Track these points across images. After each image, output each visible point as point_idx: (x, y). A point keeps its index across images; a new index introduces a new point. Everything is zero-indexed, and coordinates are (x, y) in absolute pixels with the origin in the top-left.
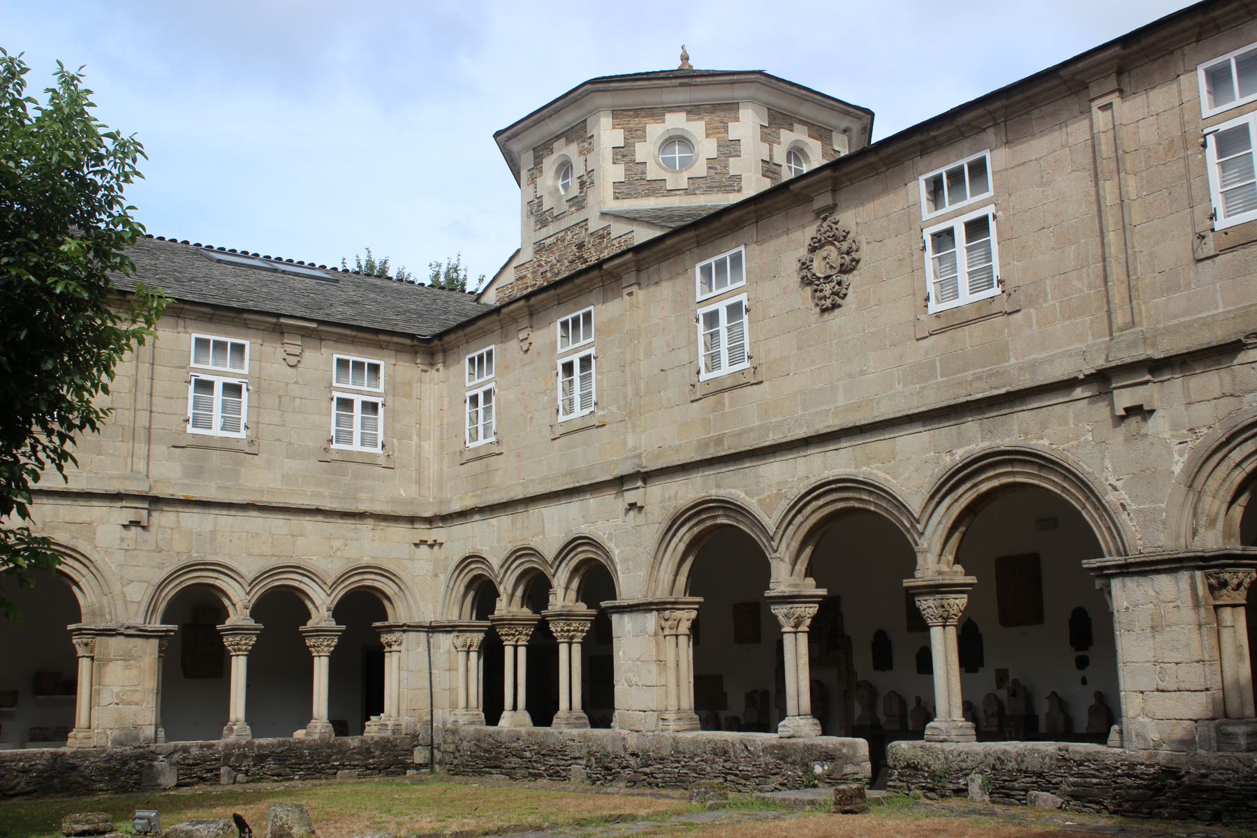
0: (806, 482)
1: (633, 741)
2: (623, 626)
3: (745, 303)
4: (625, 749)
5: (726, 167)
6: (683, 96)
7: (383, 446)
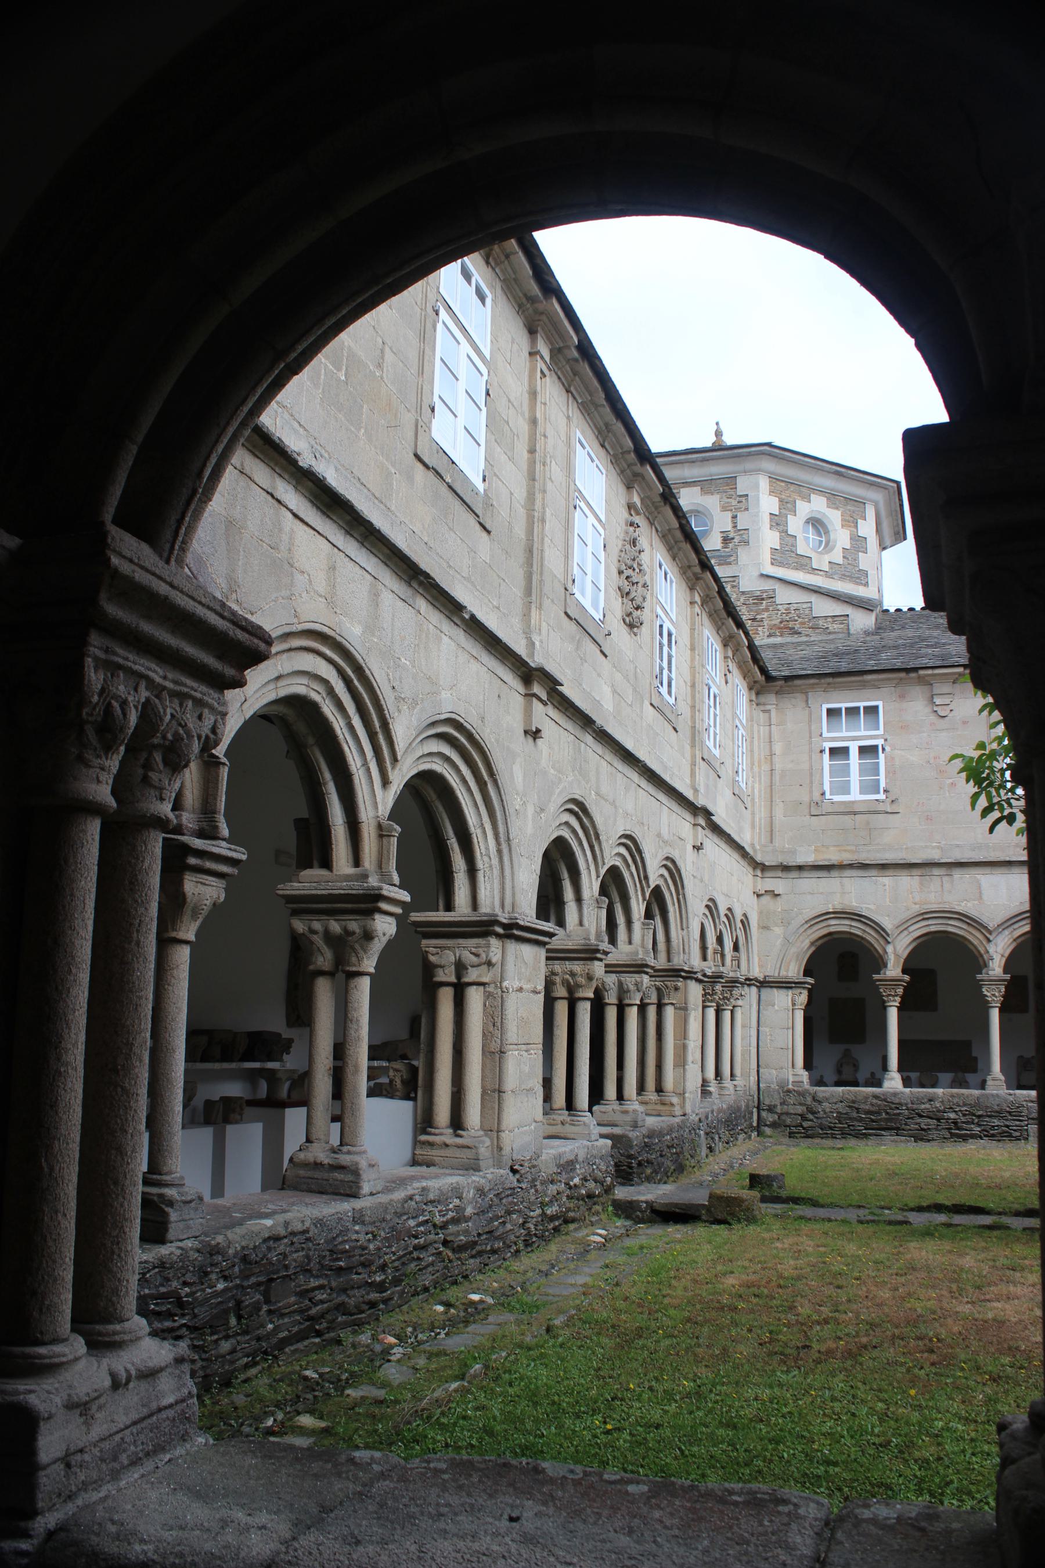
5: (856, 559)
6: (829, 482)
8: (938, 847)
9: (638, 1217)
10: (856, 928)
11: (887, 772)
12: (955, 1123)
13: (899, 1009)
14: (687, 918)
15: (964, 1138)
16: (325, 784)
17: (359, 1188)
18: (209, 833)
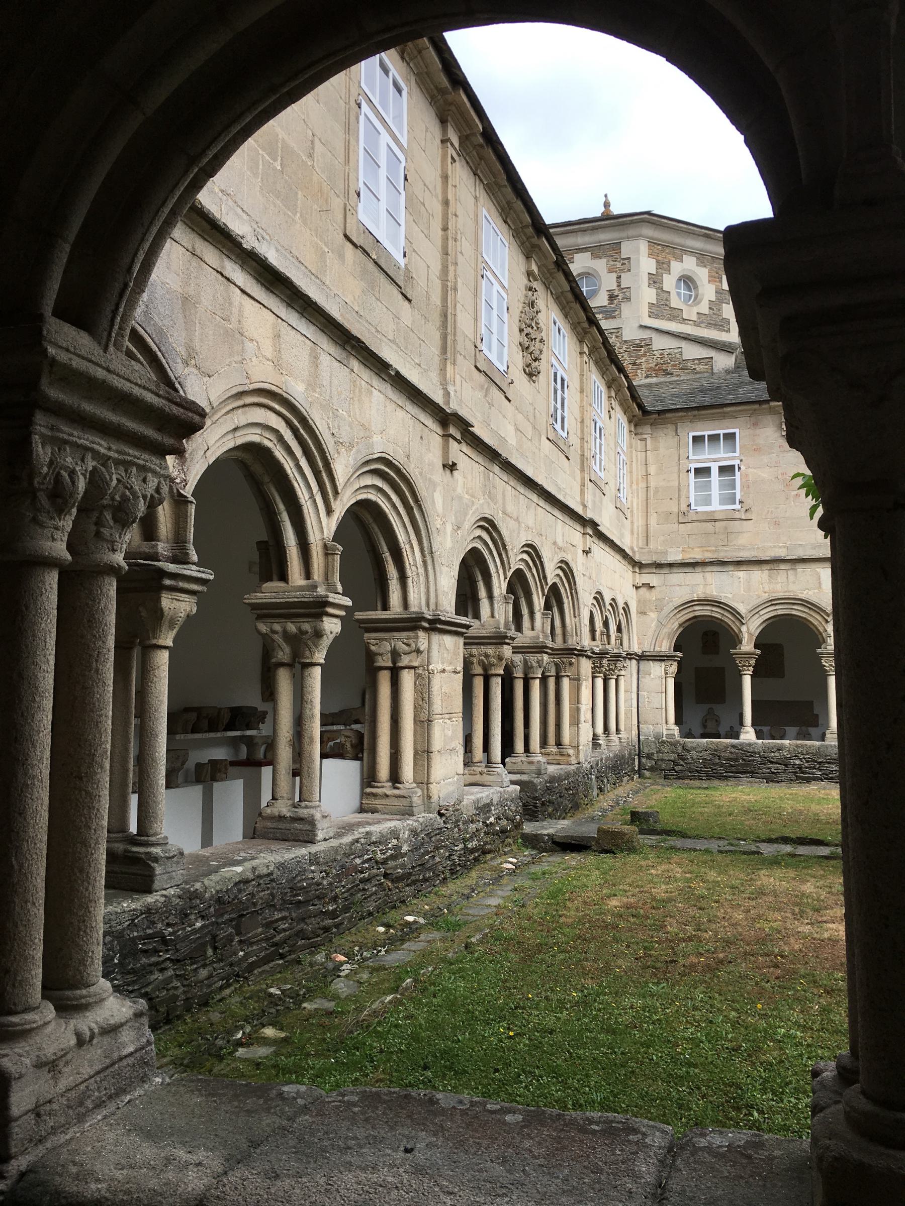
8: (784, 547)
9: (541, 847)
10: (717, 613)
11: (742, 487)
12: (800, 768)
14: (579, 608)
15: (808, 780)
16: (280, 514)
17: (315, 835)
18: (181, 558)
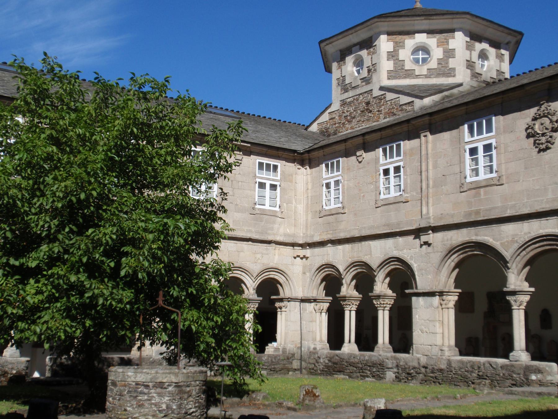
0: (529, 235)
1: (424, 360)
2: (418, 303)
3: (494, 144)
4: (419, 363)
5: (447, 63)
7: (280, 207)
13: (358, 312)
